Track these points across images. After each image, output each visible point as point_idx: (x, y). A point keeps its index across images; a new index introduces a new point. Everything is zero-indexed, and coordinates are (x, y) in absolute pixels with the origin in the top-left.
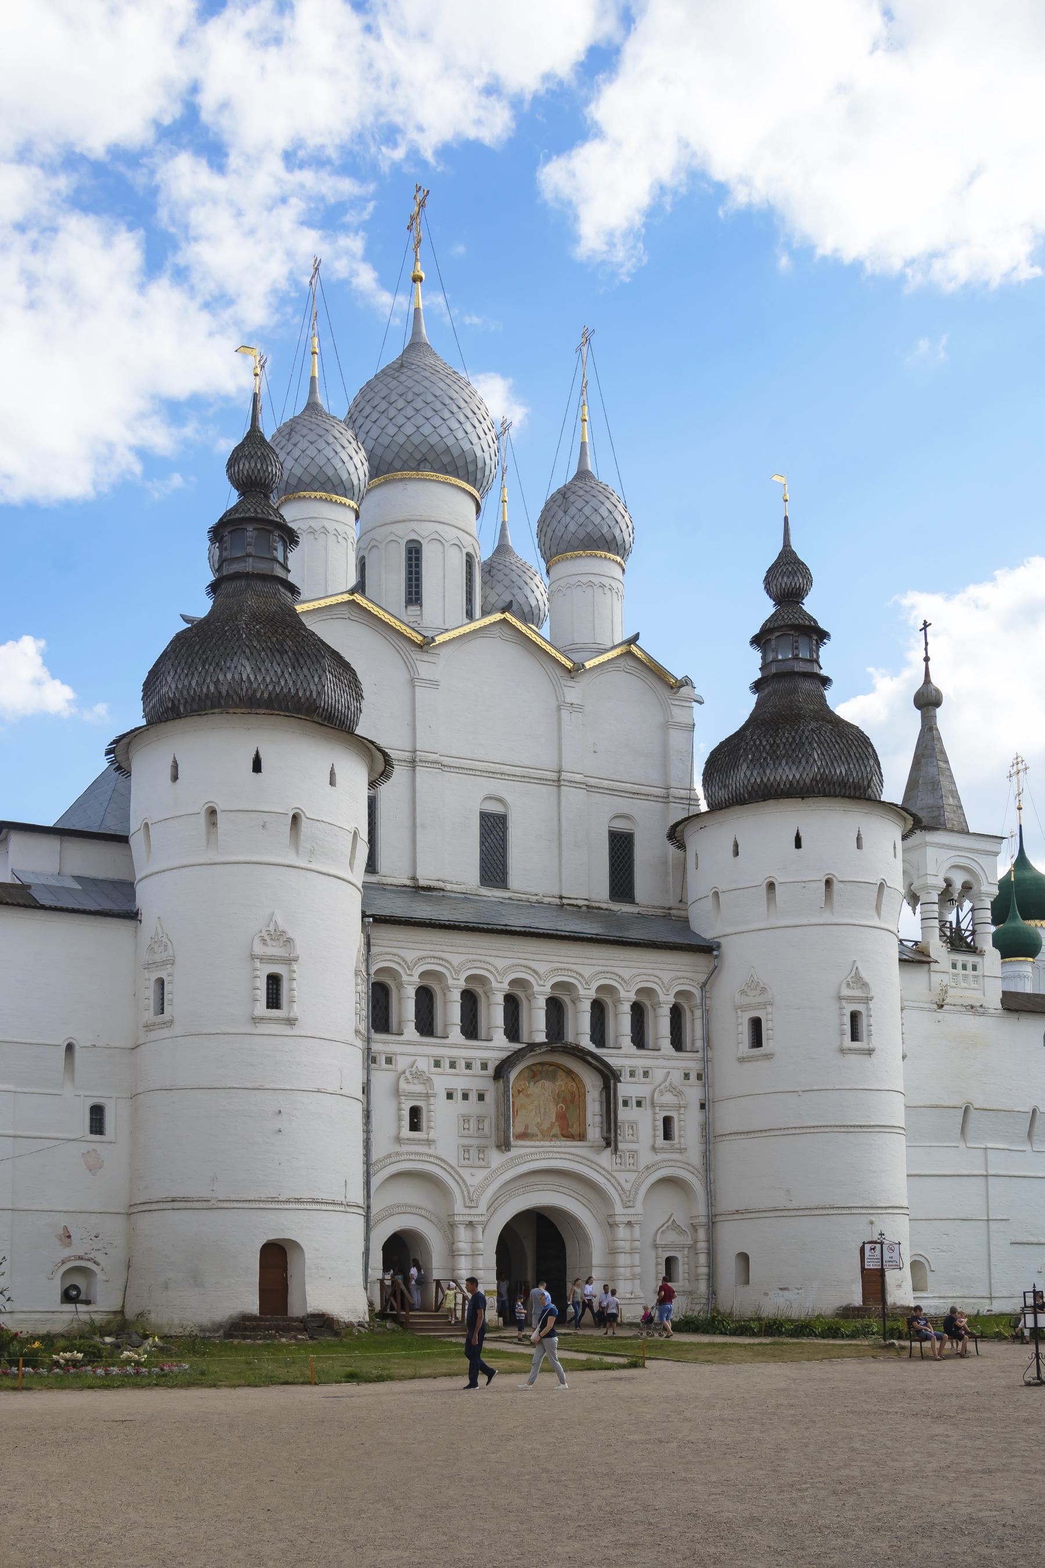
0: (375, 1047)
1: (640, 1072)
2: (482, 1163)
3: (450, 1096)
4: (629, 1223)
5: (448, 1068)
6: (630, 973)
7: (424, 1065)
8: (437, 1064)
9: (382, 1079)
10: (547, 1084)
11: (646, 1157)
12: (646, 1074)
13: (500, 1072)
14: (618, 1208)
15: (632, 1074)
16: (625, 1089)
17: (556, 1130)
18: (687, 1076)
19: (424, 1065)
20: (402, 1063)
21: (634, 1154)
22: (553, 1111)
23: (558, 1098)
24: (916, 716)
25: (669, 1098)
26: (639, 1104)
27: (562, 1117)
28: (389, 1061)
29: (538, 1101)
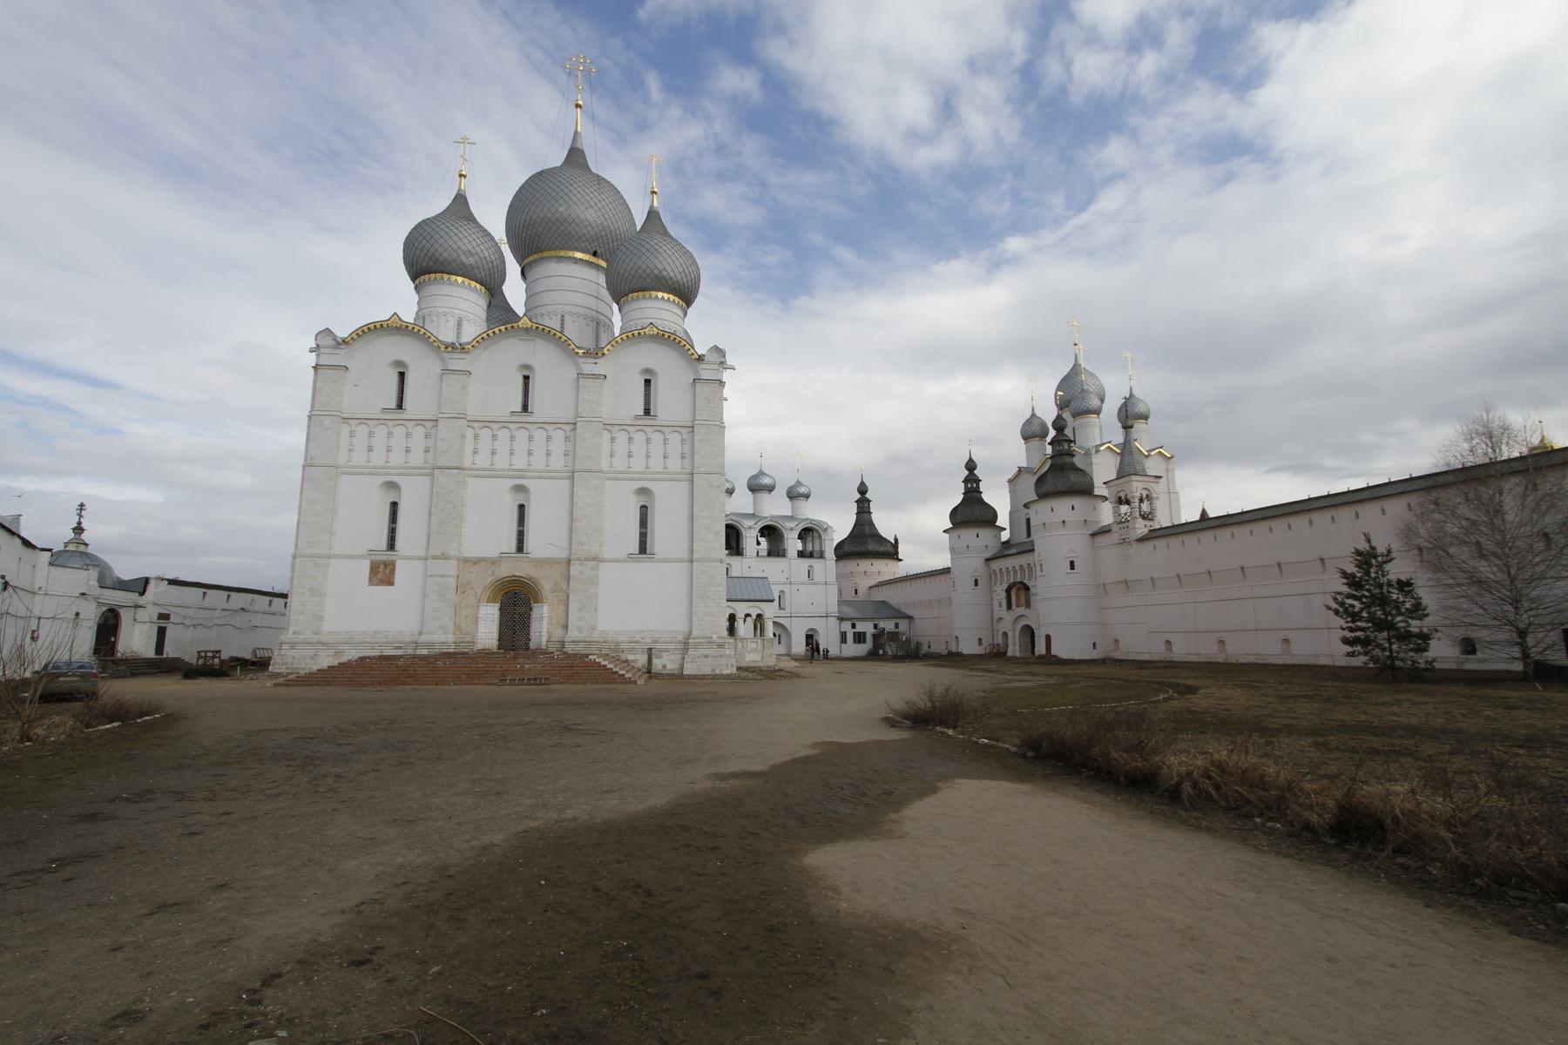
5: (1000, 590)
13: (1008, 591)
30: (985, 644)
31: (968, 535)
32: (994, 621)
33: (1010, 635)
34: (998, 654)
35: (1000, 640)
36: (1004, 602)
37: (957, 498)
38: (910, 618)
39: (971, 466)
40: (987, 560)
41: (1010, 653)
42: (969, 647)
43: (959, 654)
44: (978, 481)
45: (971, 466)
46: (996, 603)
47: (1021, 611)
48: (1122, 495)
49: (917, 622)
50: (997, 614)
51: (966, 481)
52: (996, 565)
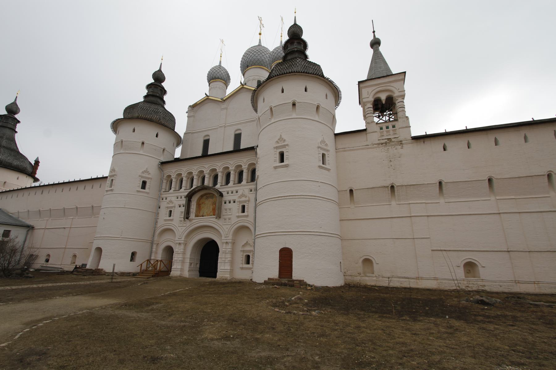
0: (163, 196)
1: (234, 192)
2: (185, 225)
3: (180, 206)
4: (227, 243)
5: (176, 199)
6: (232, 163)
7: (174, 199)
8: (177, 198)
9: (164, 204)
10: (211, 200)
11: (234, 220)
12: (237, 192)
13: (189, 197)
14: (223, 238)
15: (232, 193)
16: (226, 197)
17: (212, 214)
18: (251, 191)
19: (174, 199)
20: (169, 199)
21: (230, 219)
22: (211, 207)
23: (214, 203)
24: (371, 51)
25: (243, 199)
26: (234, 202)
27: (214, 210)
28: (166, 199)
29: (208, 205)
30: (139, 259)
31: (146, 132)
32: (157, 231)
33: (177, 250)
34: (161, 272)
35: (159, 255)
36: (179, 212)
37: (138, 95)
38: (30, 228)
39: (159, 77)
40: (163, 163)
41: (175, 272)
42: (115, 261)
43: (97, 272)
44: (164, 92)
45: (159, 77)
46: (164, 213)
47: (209, 220)
48: (383, 97)
49: (38, 234)
50: (162, 223)
51: (149, 87)
52: (173, 171)
